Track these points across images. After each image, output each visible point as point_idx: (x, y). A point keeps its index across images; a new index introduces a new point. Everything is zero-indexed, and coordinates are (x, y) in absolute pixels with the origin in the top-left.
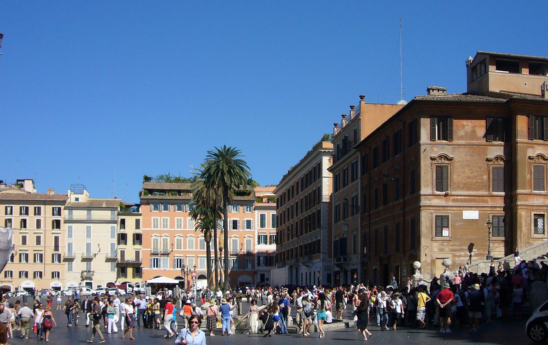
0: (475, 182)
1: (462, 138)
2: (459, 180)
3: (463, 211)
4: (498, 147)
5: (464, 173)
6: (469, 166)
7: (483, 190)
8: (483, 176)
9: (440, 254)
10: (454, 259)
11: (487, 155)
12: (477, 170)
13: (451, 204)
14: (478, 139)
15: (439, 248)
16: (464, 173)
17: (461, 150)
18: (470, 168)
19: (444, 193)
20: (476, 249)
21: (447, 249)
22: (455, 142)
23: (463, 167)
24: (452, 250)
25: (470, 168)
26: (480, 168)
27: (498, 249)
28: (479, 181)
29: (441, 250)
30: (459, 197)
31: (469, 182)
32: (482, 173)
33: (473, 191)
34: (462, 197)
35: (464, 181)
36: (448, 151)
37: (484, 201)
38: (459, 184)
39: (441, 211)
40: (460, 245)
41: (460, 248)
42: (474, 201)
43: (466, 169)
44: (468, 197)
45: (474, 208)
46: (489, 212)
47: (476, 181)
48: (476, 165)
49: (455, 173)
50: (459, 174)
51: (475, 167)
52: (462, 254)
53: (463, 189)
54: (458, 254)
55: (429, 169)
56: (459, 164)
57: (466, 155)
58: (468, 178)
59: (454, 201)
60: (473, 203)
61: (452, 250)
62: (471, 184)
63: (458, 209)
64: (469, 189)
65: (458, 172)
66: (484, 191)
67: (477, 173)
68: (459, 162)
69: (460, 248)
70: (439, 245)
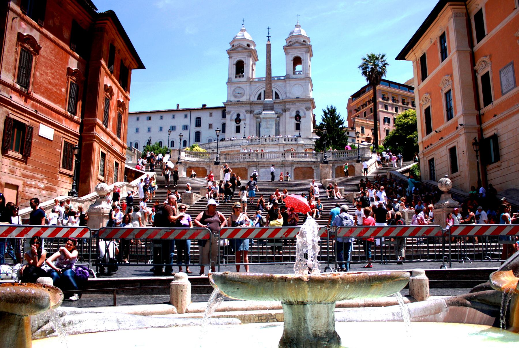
0: (55, 91)
3: (41, 124)
5: (47, 74)
6: (52, 68)
7: (60, 104)
8: (62, 88)
9: (10, 177)
10: (24, 189)
11: (67, 64)
12: (58, 77)
15: (10, 168)
16: (47, 74)
18: (53, 71)
20: (47, 181)
21: (18, 172)
23: (47, 67)
25: (53, 71)
26: (61, 77)
28: (58, 92)
29: (12, 172)
31: (50, 89)
32: (62, 84)
33: (52, 101)
35: (45, 85)
38: (40, 86)
39: (18, 115)
40: (33, 171)
41: (31, 174)
43: (49, 71)
47: (56, 90)
48: (58, 71)
49: (38, 70)
50: (43, 73)
51: (56, 72)
52: (33, 183)
53: (42, 94)
54: (29, 183)
55: (14, 49)
57: (51, 53)
58: (50, 83)
60: (49, 117)
62: (51, 91)
65: (42, 70)
66: (61, 106)
67: (57, 81)
68: (44, 57)
69: (31, 174)
70: (10, 164)
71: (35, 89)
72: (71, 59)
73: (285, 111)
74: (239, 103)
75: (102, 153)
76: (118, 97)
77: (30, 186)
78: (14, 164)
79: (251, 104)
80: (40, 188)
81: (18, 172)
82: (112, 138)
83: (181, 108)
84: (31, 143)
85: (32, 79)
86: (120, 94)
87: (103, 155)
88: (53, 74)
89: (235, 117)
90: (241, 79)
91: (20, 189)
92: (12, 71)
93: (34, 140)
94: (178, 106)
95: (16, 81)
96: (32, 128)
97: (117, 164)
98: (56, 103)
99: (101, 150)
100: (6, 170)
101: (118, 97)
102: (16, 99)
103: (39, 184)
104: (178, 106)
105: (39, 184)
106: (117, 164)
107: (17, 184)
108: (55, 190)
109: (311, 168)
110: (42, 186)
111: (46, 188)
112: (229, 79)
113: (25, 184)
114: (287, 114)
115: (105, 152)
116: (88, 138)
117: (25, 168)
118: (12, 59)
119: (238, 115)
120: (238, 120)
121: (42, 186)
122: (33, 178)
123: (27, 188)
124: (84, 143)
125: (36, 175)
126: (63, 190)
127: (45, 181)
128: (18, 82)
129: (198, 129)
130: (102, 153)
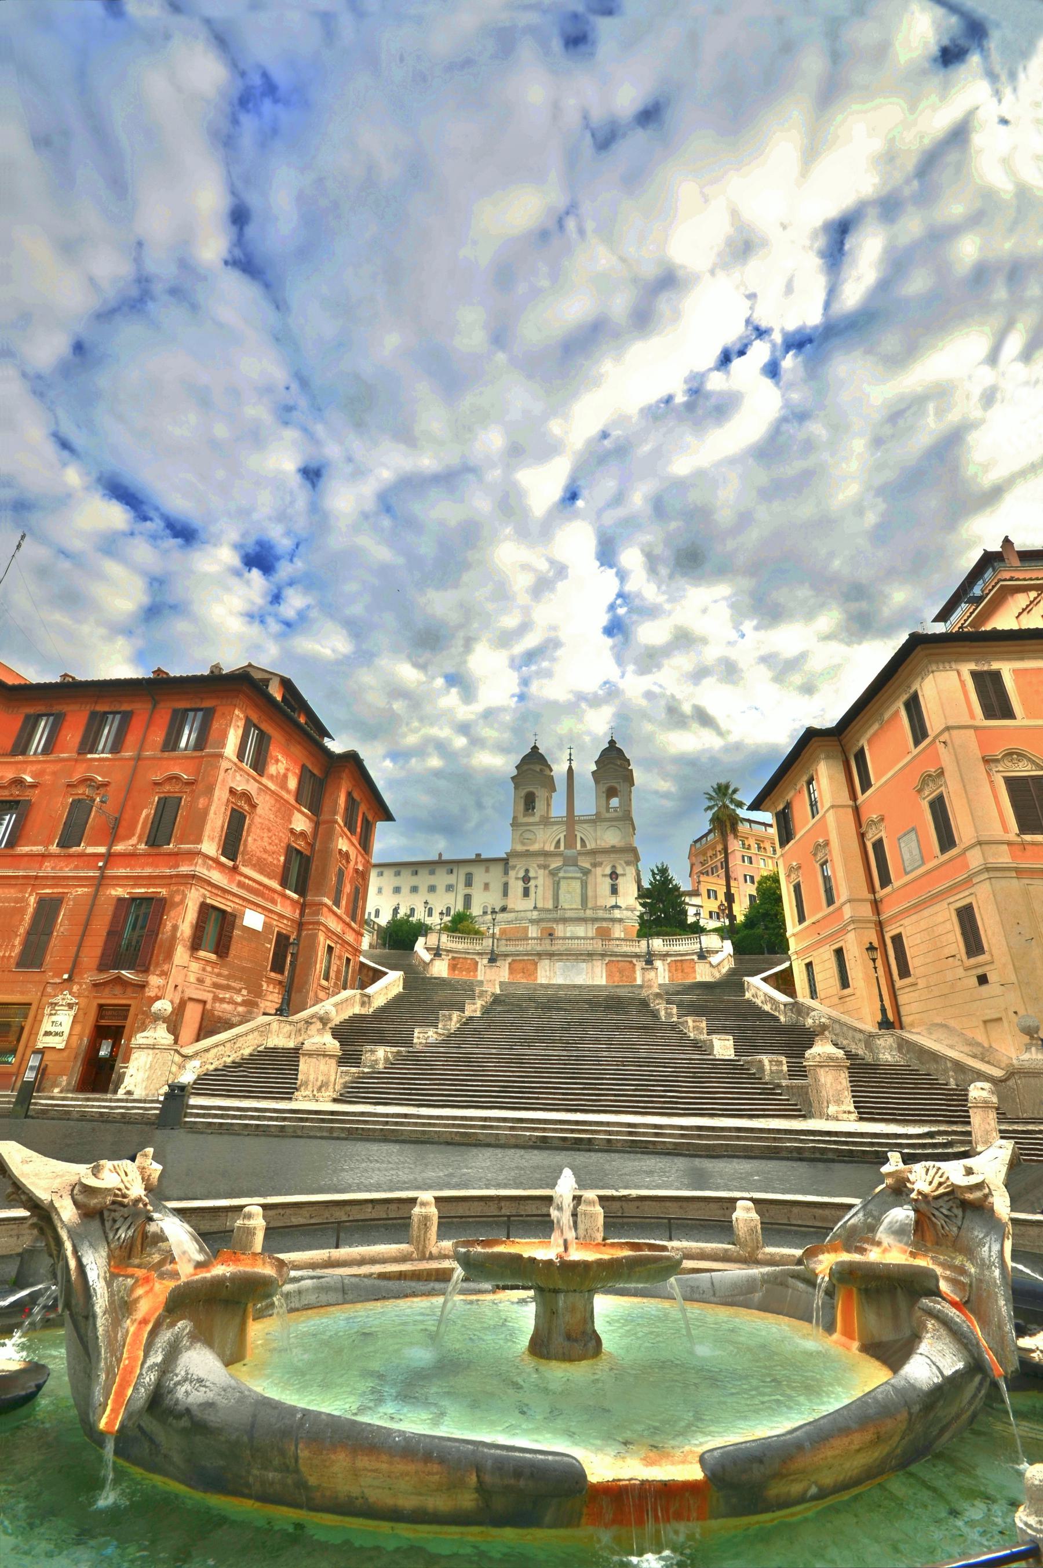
1: (271, 777)
2: (253, 848)
4: (304, 818)
6: (269, 830)
9: (197, 989)
13: (235, 889)
14: (288, 791)
17: (268, 797)
19: (231, 864)
21: (208, 981)
22: (265, 780)
24: (216, 986)
26: (280, 841)
27: (270, 998)
30: (247, 881)
33: (265, 876)
34: (250, 883)
35: (258, 854)
36: (252, 788)
37: (274, 903)
39: (219, 899)
40: (228, 978)
42: (261, 895)
43: (265, 835)
44: (257, 886)
45: (260, 910)
46: (275, 923)
52: (227, 996)
55: (223, 808)
56: (259, 820)
58: (265, 851)
59: (241, 885)
61: (216, 986)
63: (241, 902)
64: (261, 872)
71: (244, 861)
72: (297, 816)
73: (595, 865)
74: (528, 854)
75: (329, 946)
76: (356, 863)
77: (222, 1000)
78: (204, 970)
79: (546, 854)
80: (236, 1004)
81: (208, 981)
82: (344, 922)
83: (444, 858)
84: (231, 937)
85: (241, 848)
86: (360, 858)
87: (330, 949)
88: (270, 838)
89: (521, 874)
90: (531, 820)
91: (208, 1006)
92: (217, 839)
93: (237, 932)
94: (440, 855)
95: (220, 852)
96: (235, 916)
97: (348, 960)
98: (270, 878)
99: (328, 942)
100: (192, 978)
101: (356, 863)
102: (217, 877)
103: (235, 997)
104: (440, 855)
105: (235, 997)
106: (348, 960)
107: (204, 998)
108: (258, 1005)
109: (631, 962)
110: (239, 999)
111: (244, 1003)
112: (515, 818)
113: (216, 999)
114: (599, 871)
115: (333, 945)
116: (311, 927)
117: (219, 975)
118: (219, 823)
119: (527, 871)
120: (526, 879)
121: (239, 999)
122: (227, 988)
123: (217, 1005)
124: (304, 933)
125: (233, 984)
126: (269, 1004)
127: (244, 992)
128: (223, 854)
129: (468, 891)
130: (329, 946)
